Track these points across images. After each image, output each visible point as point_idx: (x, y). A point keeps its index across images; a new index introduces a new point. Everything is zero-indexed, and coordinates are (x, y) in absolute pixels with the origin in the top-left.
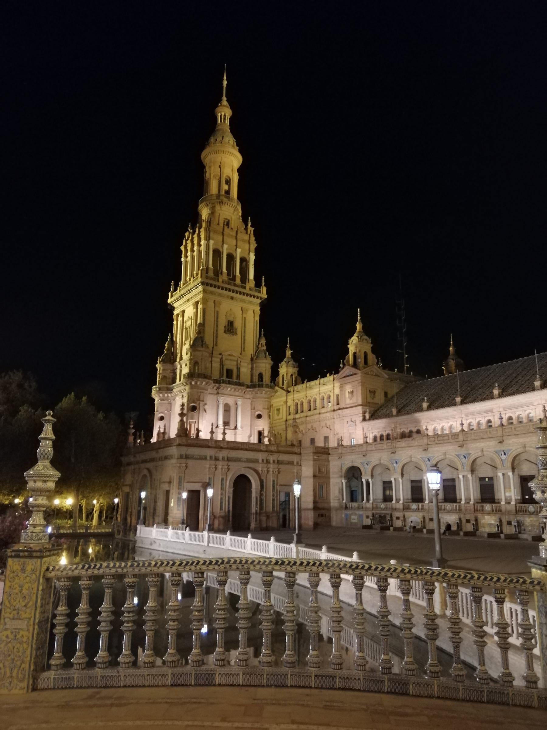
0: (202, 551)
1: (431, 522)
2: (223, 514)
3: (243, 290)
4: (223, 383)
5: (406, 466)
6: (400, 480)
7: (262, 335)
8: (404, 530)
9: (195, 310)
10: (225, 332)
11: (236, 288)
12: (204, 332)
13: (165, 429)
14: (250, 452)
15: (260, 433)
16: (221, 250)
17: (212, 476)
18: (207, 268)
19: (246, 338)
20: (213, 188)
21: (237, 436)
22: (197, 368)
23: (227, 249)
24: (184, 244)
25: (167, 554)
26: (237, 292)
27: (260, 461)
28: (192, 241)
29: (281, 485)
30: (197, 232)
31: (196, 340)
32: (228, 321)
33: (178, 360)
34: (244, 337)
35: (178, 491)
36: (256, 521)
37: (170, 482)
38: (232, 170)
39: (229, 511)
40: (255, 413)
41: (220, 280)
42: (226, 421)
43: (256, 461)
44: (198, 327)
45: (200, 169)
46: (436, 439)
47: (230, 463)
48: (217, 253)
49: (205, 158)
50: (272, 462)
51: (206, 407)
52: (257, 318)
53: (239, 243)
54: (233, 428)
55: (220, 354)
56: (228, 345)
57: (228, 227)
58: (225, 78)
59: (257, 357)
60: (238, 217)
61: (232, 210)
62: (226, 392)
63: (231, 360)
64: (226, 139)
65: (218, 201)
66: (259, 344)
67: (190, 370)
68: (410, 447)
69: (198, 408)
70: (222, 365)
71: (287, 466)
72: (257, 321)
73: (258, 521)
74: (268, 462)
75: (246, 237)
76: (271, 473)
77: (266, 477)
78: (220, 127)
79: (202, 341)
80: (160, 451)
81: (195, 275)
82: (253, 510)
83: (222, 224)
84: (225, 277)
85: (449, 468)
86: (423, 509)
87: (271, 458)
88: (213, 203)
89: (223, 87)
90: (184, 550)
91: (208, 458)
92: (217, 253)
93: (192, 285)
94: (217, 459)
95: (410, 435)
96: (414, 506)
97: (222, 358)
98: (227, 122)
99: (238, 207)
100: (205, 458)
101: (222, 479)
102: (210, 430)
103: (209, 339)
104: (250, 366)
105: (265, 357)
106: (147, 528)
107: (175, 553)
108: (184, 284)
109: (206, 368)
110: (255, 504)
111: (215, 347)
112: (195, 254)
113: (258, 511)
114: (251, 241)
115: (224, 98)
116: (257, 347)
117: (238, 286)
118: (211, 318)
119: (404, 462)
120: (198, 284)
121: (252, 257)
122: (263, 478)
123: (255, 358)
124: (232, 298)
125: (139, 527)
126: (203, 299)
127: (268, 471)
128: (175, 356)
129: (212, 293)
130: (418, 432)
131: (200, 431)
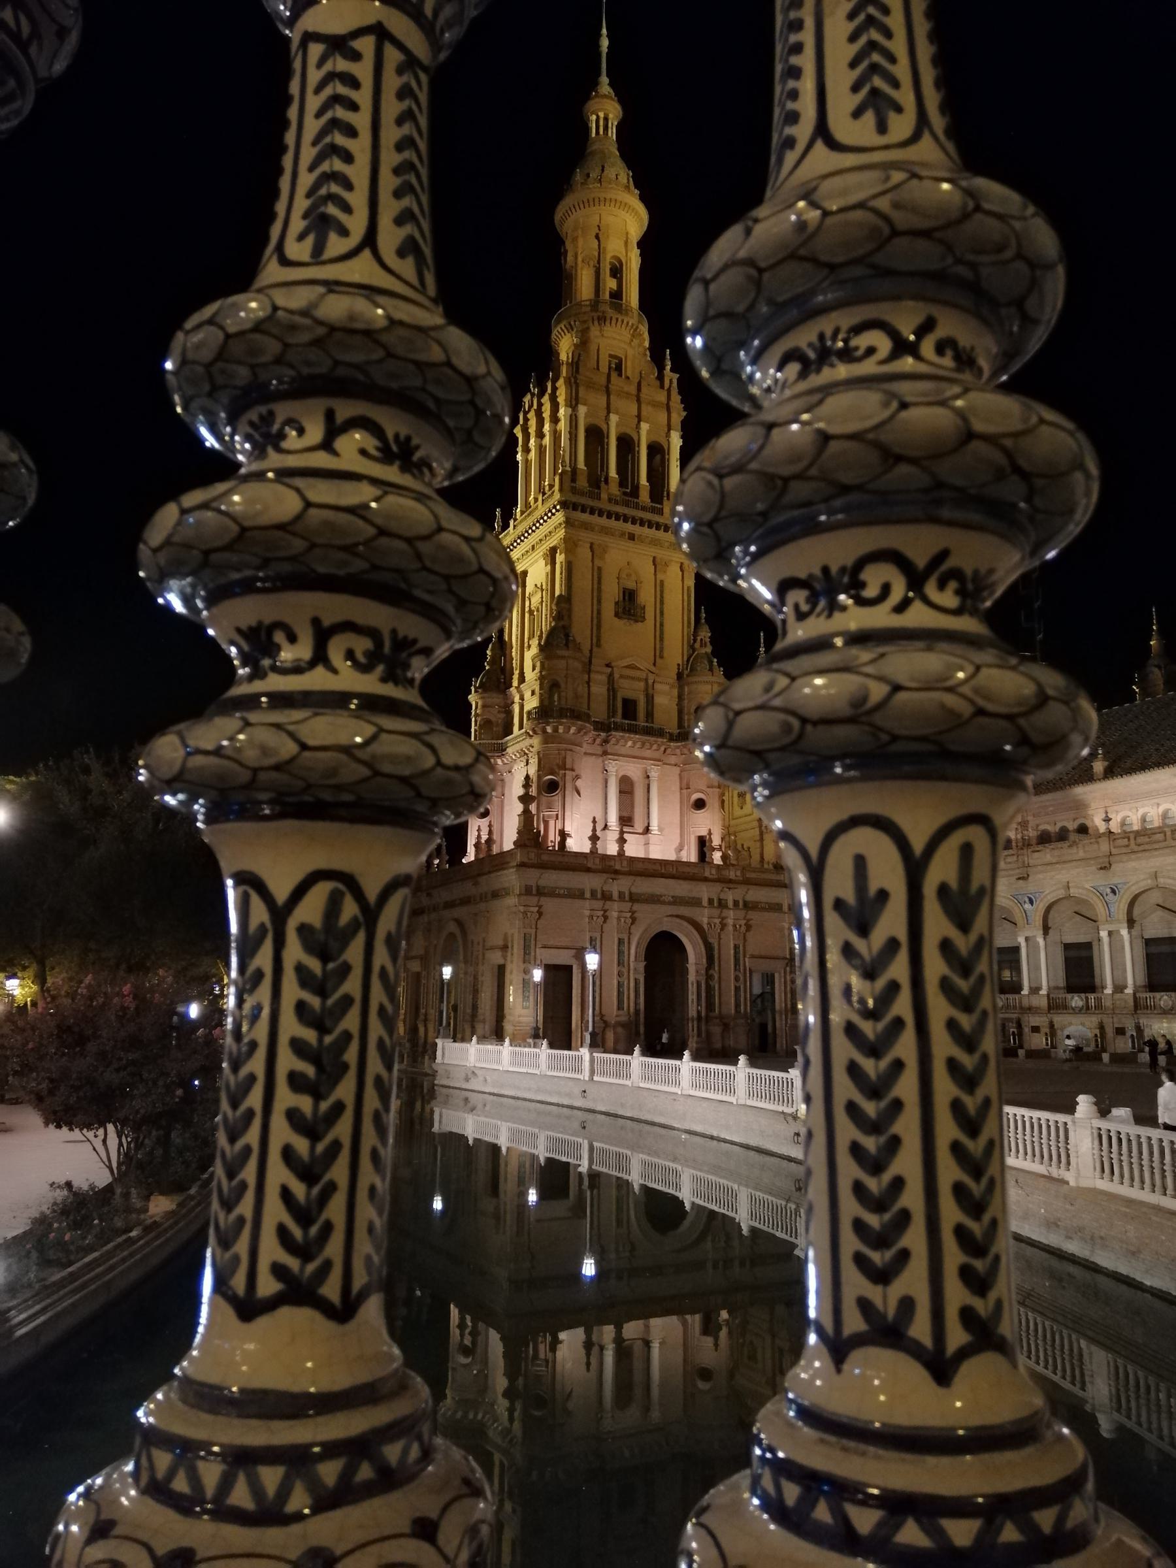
0: (577, 1091)
1: (1120, 1037)
2: (624, 1019)
3: (656, 518)
4: (616, 729)
5: (1055, 907)
6: (1041, 941)
8: (1053, 1055)
9: (549, 567)
10: (617, 615)
11: (640, 514)
12: (570, 617)
13: (490, 833)
14: (681, 882)
15: (702, 842)
16: (604, 427)
17: (598, 935)
18: (574, 470)
20: (584, 287)
21: (652, 848)
22: (556, 698)
23: (617, 425)
24: (521, 422)
25: (502, 1099)
26: (642, 524)
27: (705, 902)
28: (539, 414)
29: (753, 957)
30: (549, 391)
31: (552, 633)
32: (625, 591)
33: (515, 683)
34: (662, 625)
35: (522, 966)
36: (699, 1035)
37: (505, 948)
38: (626, 243)
39: (637, 1012)
40: (689, 796)
41: (604, 496)
42: (625, 814)
43: (696, 902)
44: (557, 604)
45: (553, 246)
46: (1132, 841)
47: (636, 907)
48: (596, 436)
49: (562, 224)
51: (579, 783)
53: (646, 410)
54: (641, 831)
55: (608, 665)
56: (626, 643)
57: (620, 375)
58: (604, 31)
60: (641, 349)
61: (626, 334)
62: (623, 751)
63: (633, 678)
64: (610, 172)
65: (595, 315)
66: (695, 640)
67: (541, 701)
68: (1064, 862)
69: (561, 784)
70: (612, 690)
71: (766, 914)
72: (689, 588)
74: (722, 904)
75: (662, 397)
76: (731, 928)
77: (720, 938)
78: (594, 147)
79: (567, 635)
80: (483, 880)
81: (547, 488)
82: (692, 1011)
83: (604, 368)
84: (614, 489)
85: (1160, 913)
86: (1099, 1006)
87: (730, 897)
88: (585, 322)
89: (599, 54)
90: (538, 1090)
91: (588, 895)
92: (596, 436)
93: (541, 509)
94: (606, 897)
95: (1063, 835)
96: (1076, 1001)
97: (611, 675)
98: (613, 133)
99: (641, 326)
100: (580, 895)
101: (621, 942)
102: (590, 833)
103: (581, 630)
104: (675, 692)
105: (711, 670)
106: (456, 1044)
107: (518, 1098)
108: (522, 513)
109: (577, 697)
110: (695, 997)
111: (595, 649)
112: (547, 440)
113: (703, 1014)
114: (671, 404)
115: (604, 79)
117: (644, 509)
118: (584, 583)
119: (1051, 898)
120: (555, 507)
122: (711, 940)
123: (686, 672)
124: (632, 537)
125: (439, 1042)
126: (566, 540)
127: (723, 926)
128: (507, 675)
129: (586, 526)
130: (1083, 830)
131: (569, 835)
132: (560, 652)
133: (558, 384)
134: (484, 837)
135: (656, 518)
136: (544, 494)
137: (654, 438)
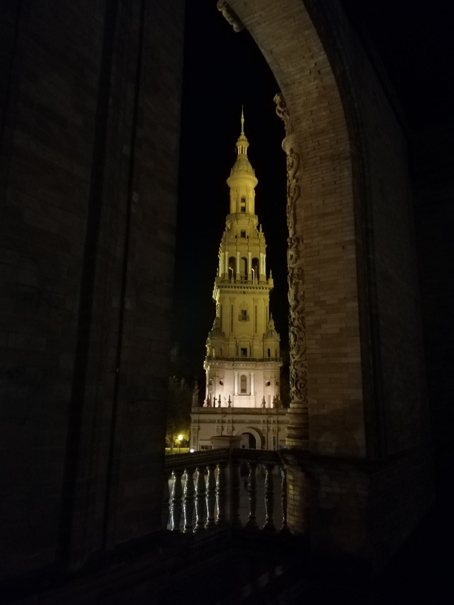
4: (236, 360)
7: (271, 318)
10: (239, 320)
27: (262, 422)
29: (281, 441)
32: (243, 311)
42: (244, 388)
43: (258, 422)
47: (235, 425)
50: (272, 422)
52: (268, 304)
55: (235, 338)
58: (243, 116)
59: (267, 336)
62: (240, 367)
72: (267, 307)
73: (260, 469)
74: (268, 422)
91: (217, 421)
94: (223, 422)
100: (214, 422)
104: (262, 344)
115: (243, 133)
116: (267, 327)
121: (263, 257)
122: (264, 435)
127: (269, 430)
132: (214, 338)
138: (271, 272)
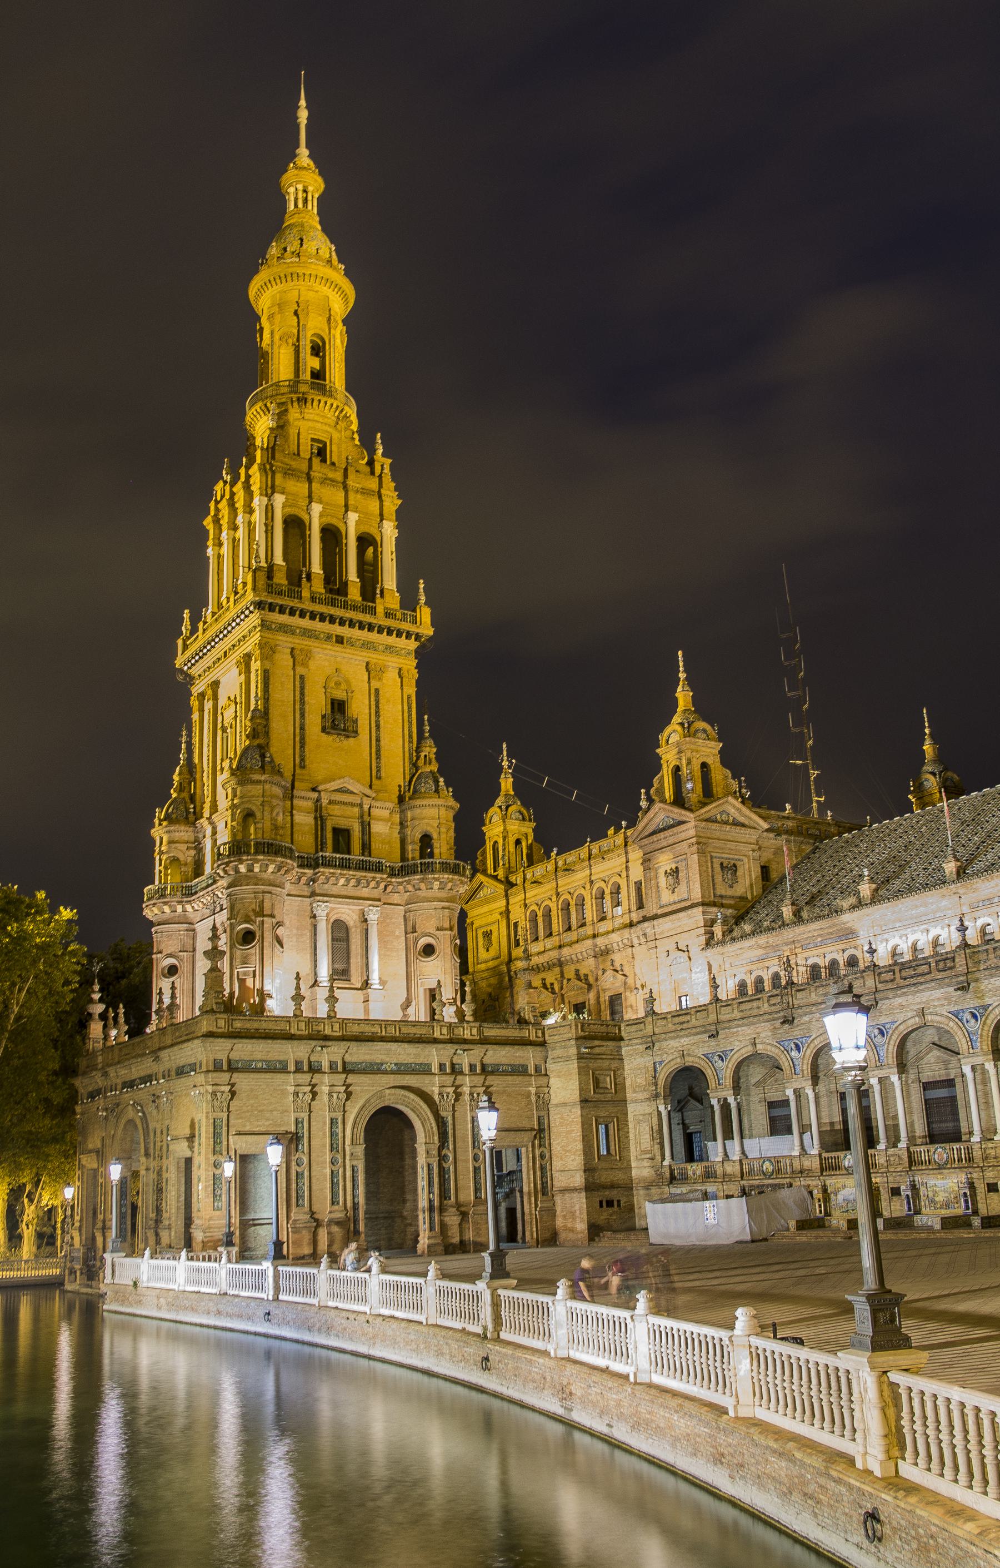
1: (895, 1198)
2: (339, 1215)
3: (367, 618)
8: (827, 1224)
9: (243, 676)
10: (324, 730)
11: (349, 614)
12: (267, 733)
13: (173, 996)
14: (406, 1045)
15: (433, 995)
16: (305, 517)
17: (305, 1116)
19: (382, 743)
20: (281, 367)
21: (371, 1005)
22: (252, 829)
23: (321, 516)
24: (212, 513)
26: (352, 624)
27: (435, 1069)
28: (232, 503)
30: (243, 478)
33: (206, 813)
34: (378, 740)
35: (212, 1159)
36: (432, 1228)
37: (191, 1139)
39: (355, 1207)
40: (416, 941)
41: (306, 594)
43: (424, 1070)
46: (898, 975)
47: (352, 1079)
48: (295, 526)
49: (257, 296)
50: (466, 1069)
51: (280, 931)
52: (411, 690)
54: (359, 986)
55: (314, 790)
57: (324, 461)
59: (414, 792)
60: (349, 433)
63: (344, 803)
64: (310, 246)
65: (295, 396)
66: (418, 758)
67: (234, 835)
69: (258, 934)
70: (320, 818)
71: (510, 1078)
72: (409, 697)
74: (455, 1070)
76: (467, 1098)
77: (454, 1111)
79: (263, 756)
80: (164, 1054)
81: (240, 587)
82: (423, 1202)
83: (305, 454)
84: (318, 586)
85: (936, 1053)
87: (465, 1060)
88: (283, 403)
92: (295, 526)
94: (314, 1069)
97: (318, 800)
98: (313, 207)
101: (333, 1122)
102: (294, 993)
104: (397, 818)
105: (437, 791)
108: (214, 614)
109: (276, 827)
110: (425, 1183)
111: (298, 771)
112: (240, 534)
113: (436, 1203)
115: (303, 152)
116: (415, 765)
117: (355, 608)
121: (389, 532)
122: (443, 1114)
123: (408, 795)
124: (340, 640)
126: (261, 645)
127: (458, 1096)
128: (198, 804)
129: (285, 629)
131: (270, 996)
132: (256, 777)
133: (250, 472)
134: (167, 1001)
135: (367, 618)
136: (236, 593)
137: (364, 529)
138: (422, 586)
